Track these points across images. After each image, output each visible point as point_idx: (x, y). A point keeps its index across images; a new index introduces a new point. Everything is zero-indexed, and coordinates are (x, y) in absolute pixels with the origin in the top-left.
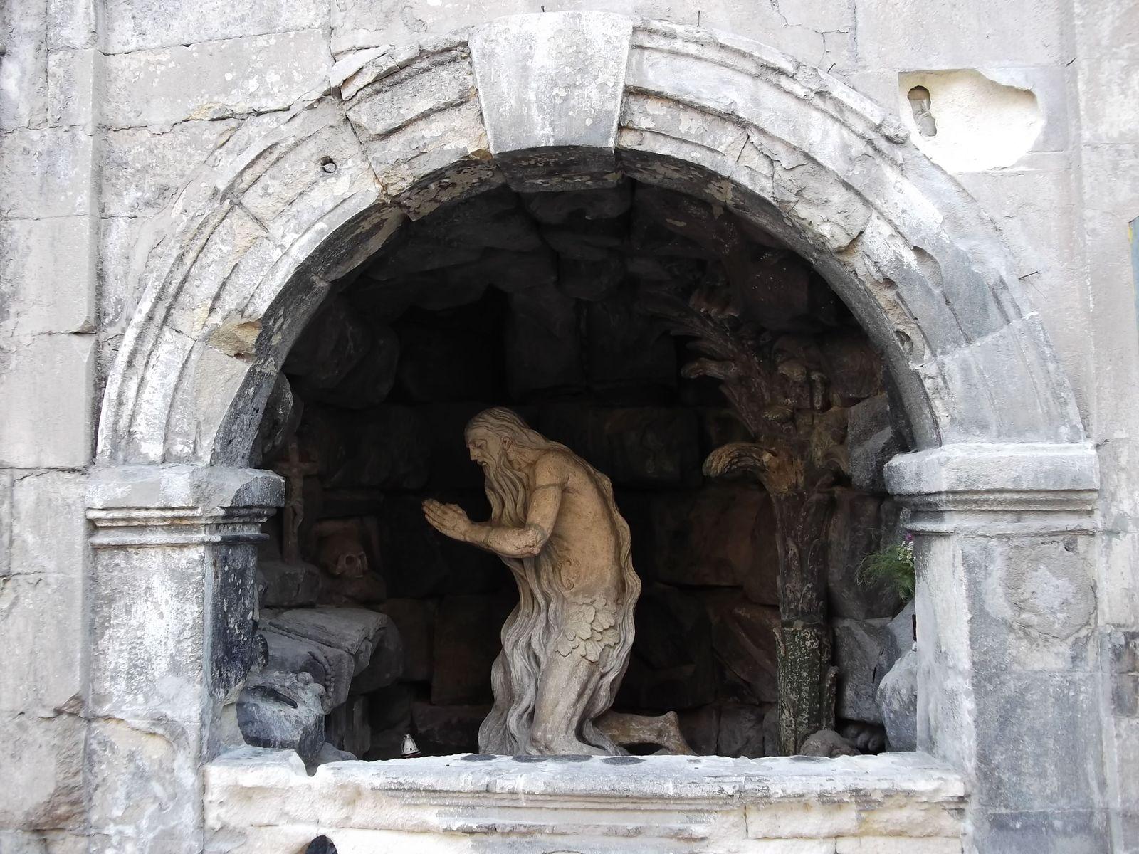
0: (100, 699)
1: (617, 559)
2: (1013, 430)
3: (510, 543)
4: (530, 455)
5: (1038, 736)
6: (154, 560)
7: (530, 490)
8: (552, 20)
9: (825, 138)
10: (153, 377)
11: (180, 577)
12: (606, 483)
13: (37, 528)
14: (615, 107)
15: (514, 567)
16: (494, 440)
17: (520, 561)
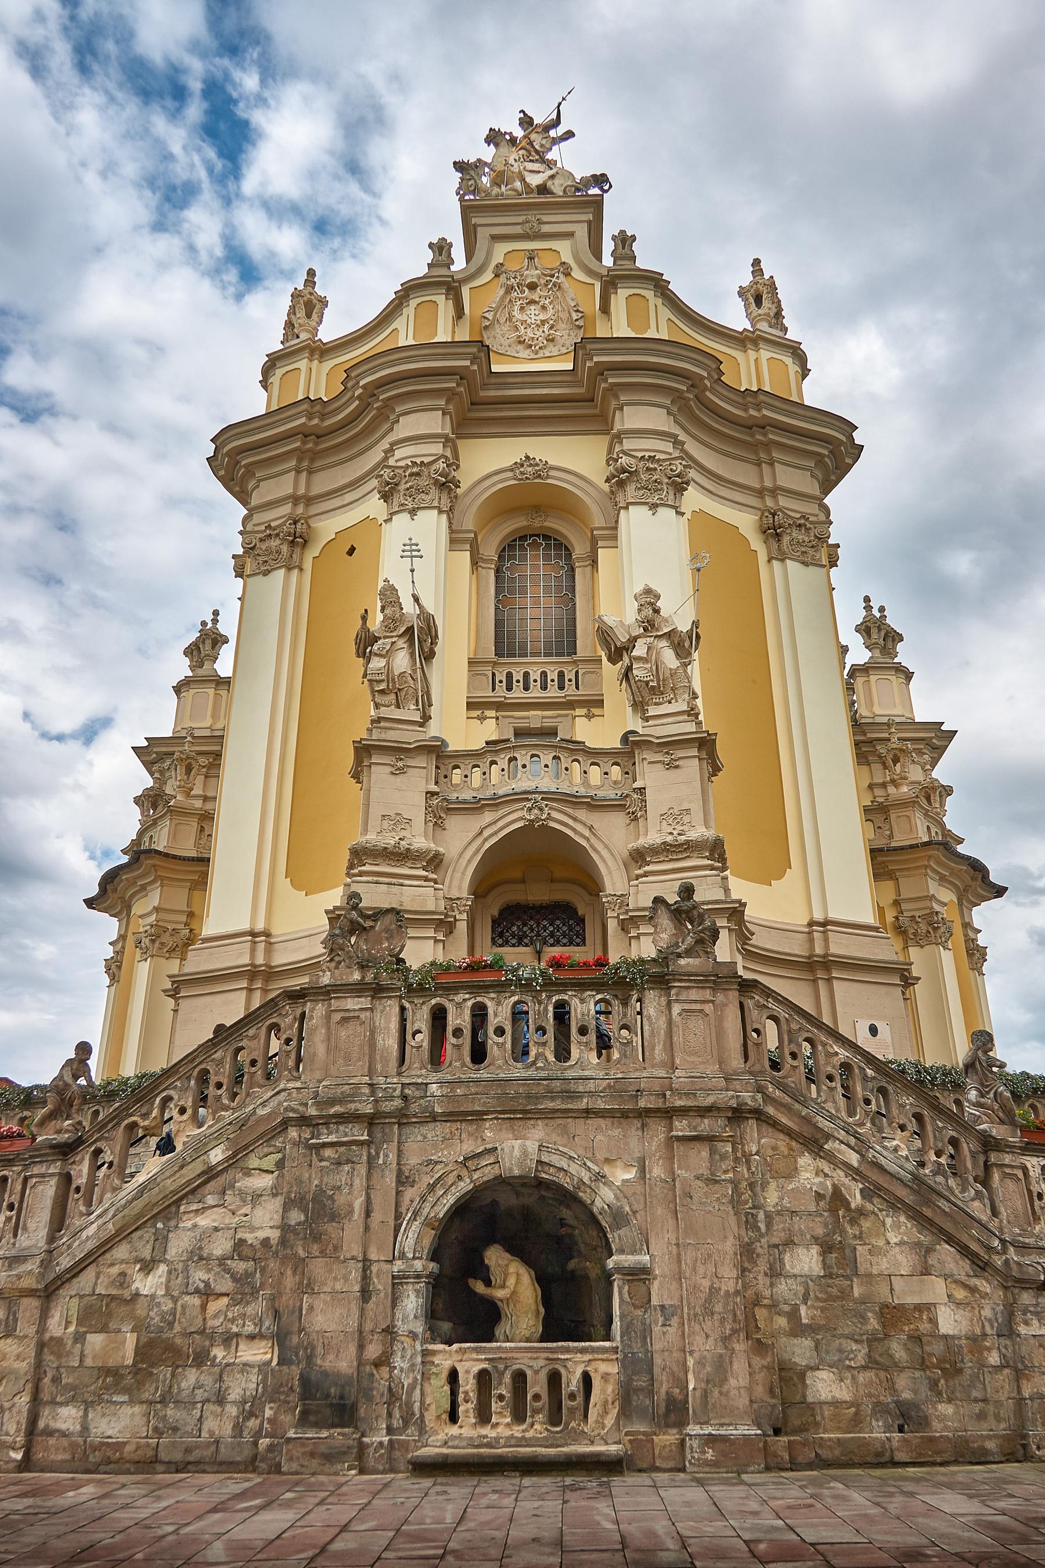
0: (395, 1326)
1: (536, 1301)
2: (633, 1252)
3: (500, 1294)
4: (506, 1262)
5: (635, 1332)
6: (410, 1287)
7: (506, 1275)
8: (519, 1141)
9: (586, 1177)
10: (410, 1235)
11: (417, 1291)
12: (533, 1273)
13: (378, 1277)
14: (534, 1166)
15: (499, 1303)
16: (495, 1257)
17: (501, 1301)
